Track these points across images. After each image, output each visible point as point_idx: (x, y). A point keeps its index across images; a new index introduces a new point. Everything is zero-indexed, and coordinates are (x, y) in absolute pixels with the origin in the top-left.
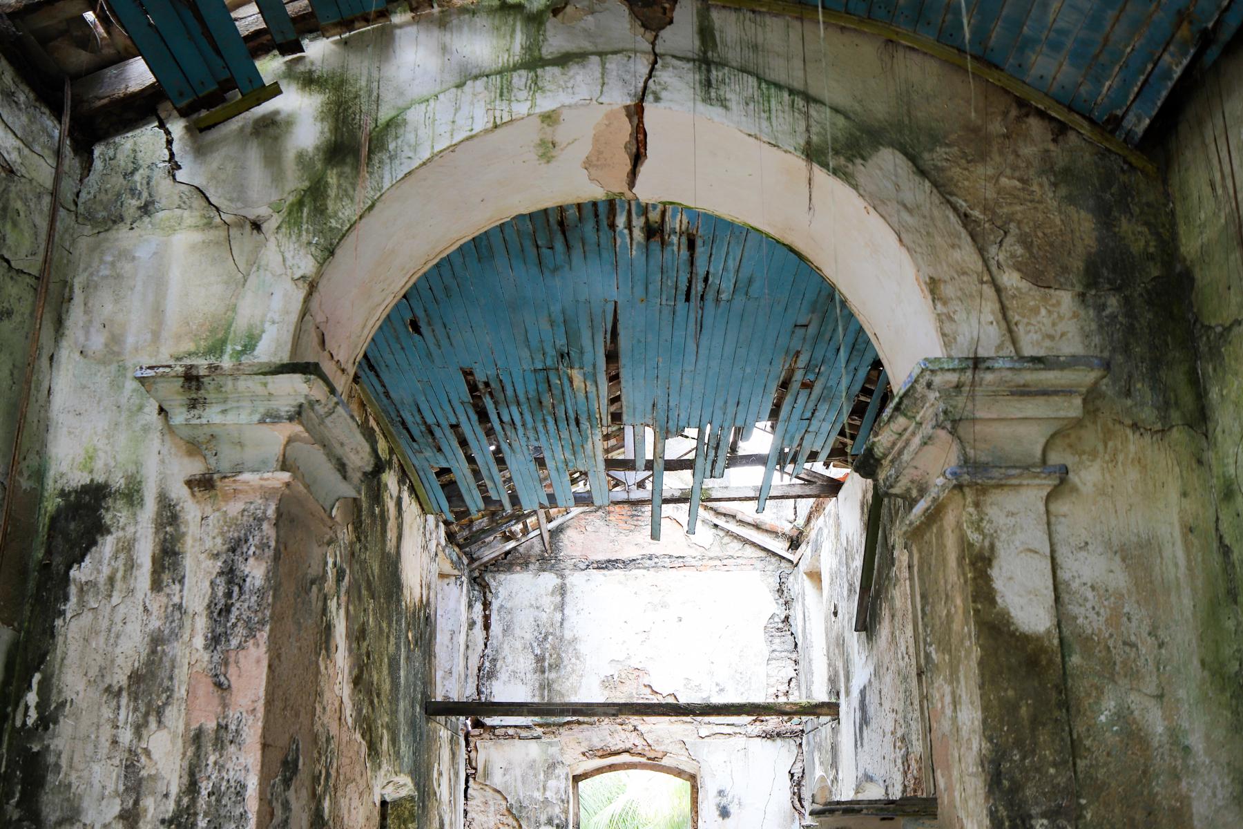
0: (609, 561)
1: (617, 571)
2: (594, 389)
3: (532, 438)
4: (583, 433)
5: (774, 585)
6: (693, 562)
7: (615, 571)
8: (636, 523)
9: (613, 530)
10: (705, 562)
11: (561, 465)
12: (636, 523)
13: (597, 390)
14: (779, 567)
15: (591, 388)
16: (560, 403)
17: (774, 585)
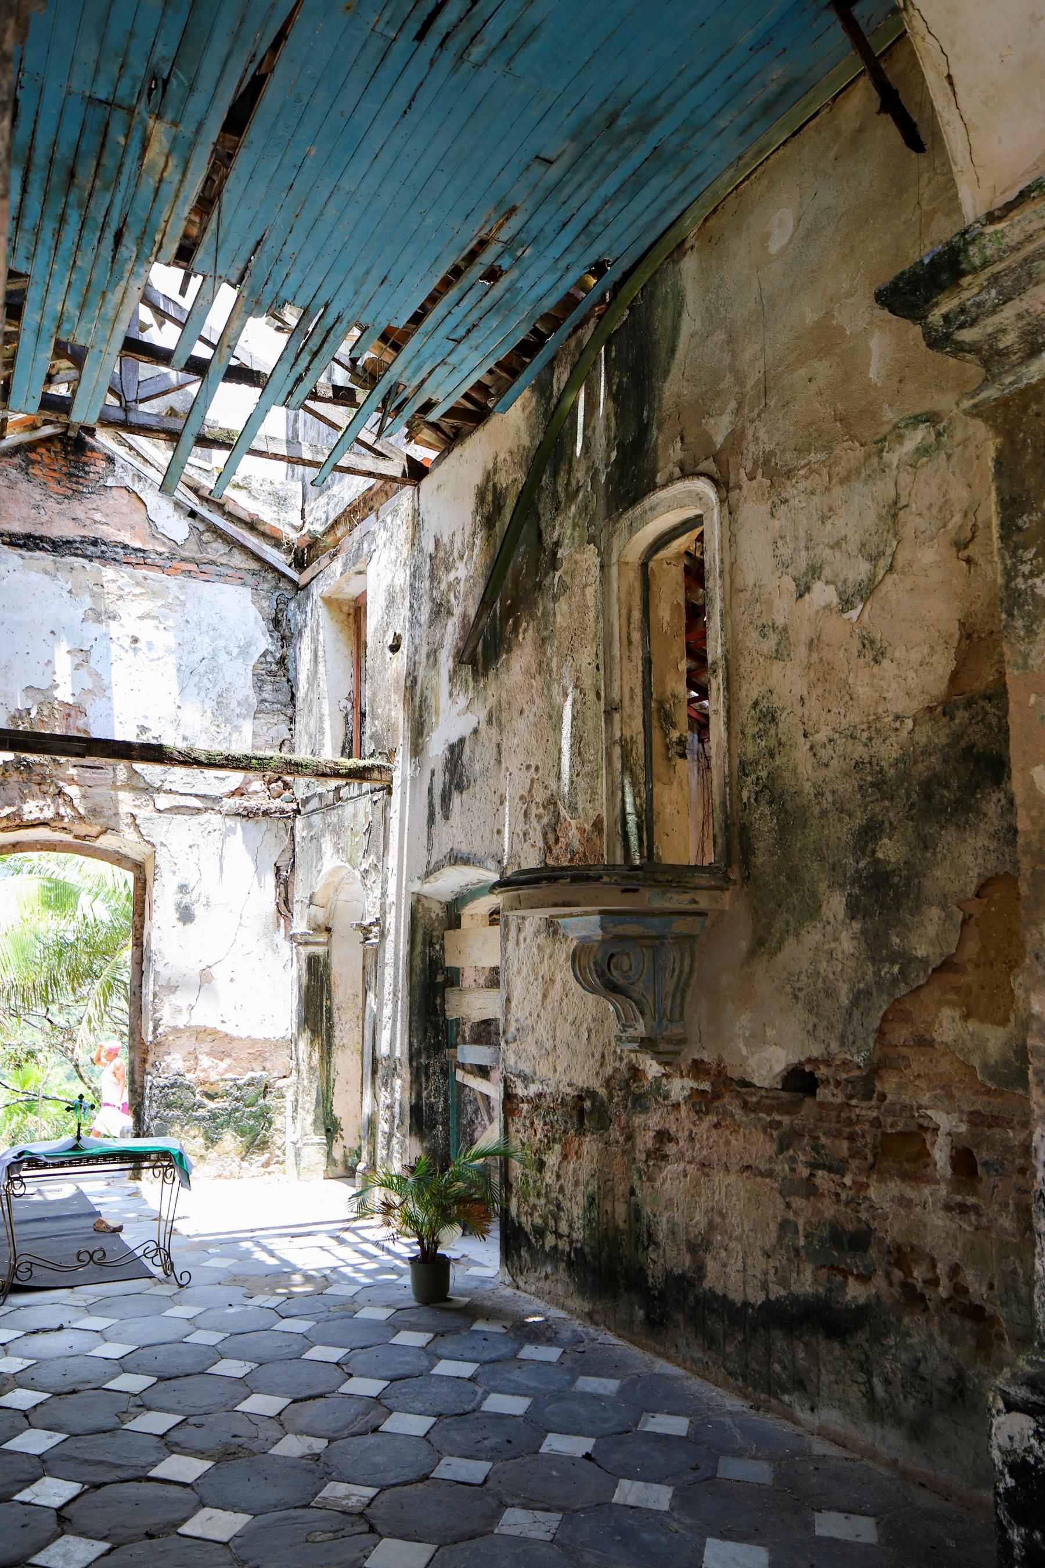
0: (29, 536)
1: (42, 554)
2: (177, 178)
3: (21, 252)
4: (116, 267)
5: (268, 610)
6: (160, 562)
7: (38, 554)
8: (75, 487)
9: (38, 490)
10: (175, 563)
11: (49, 324)
12: (75, 487)
13: (181, 181)
14: (277, 588)
15: (172, 175)
16: (106, 188)
17: (268, 610)
